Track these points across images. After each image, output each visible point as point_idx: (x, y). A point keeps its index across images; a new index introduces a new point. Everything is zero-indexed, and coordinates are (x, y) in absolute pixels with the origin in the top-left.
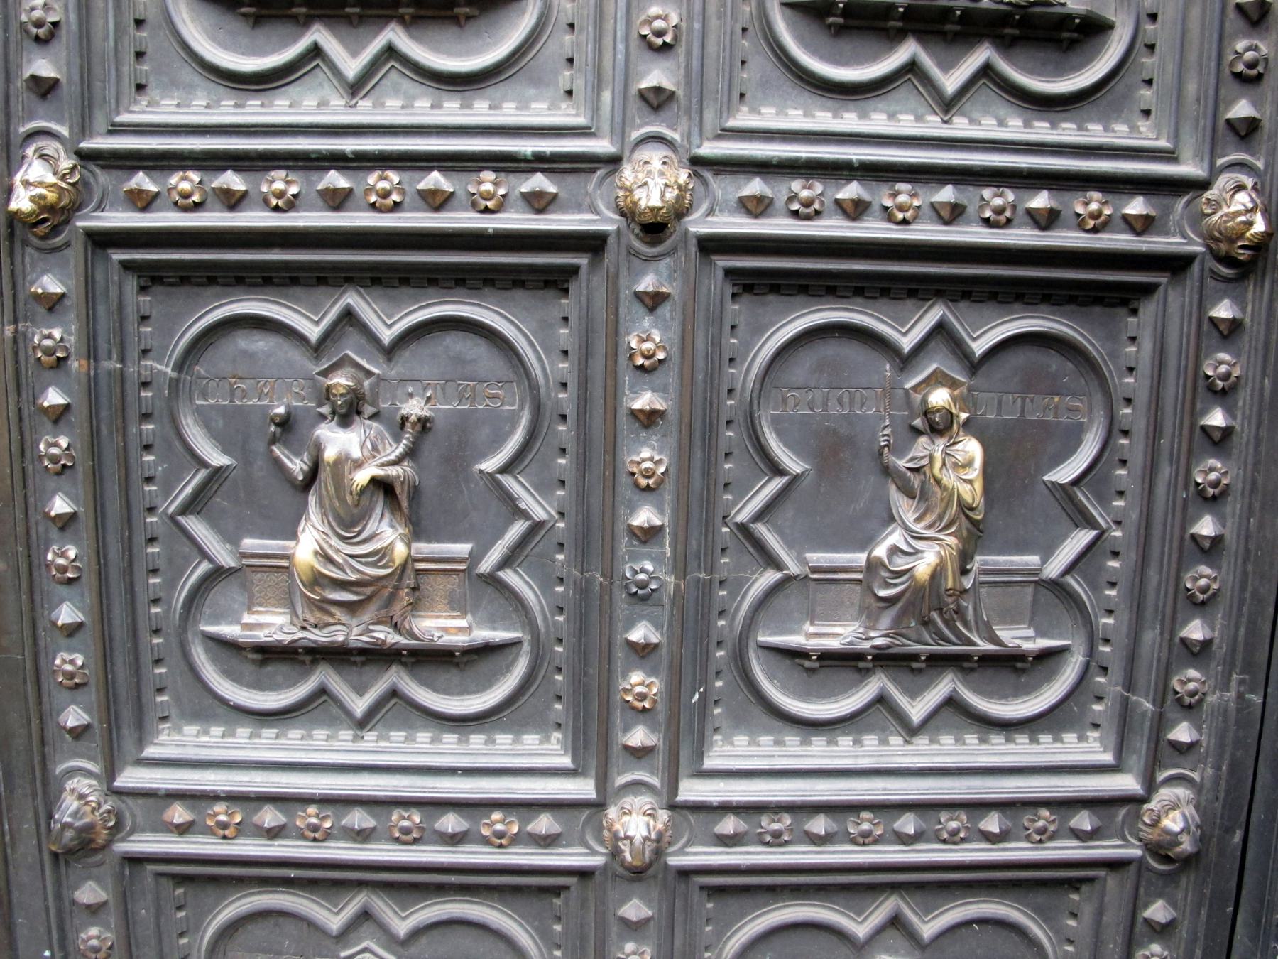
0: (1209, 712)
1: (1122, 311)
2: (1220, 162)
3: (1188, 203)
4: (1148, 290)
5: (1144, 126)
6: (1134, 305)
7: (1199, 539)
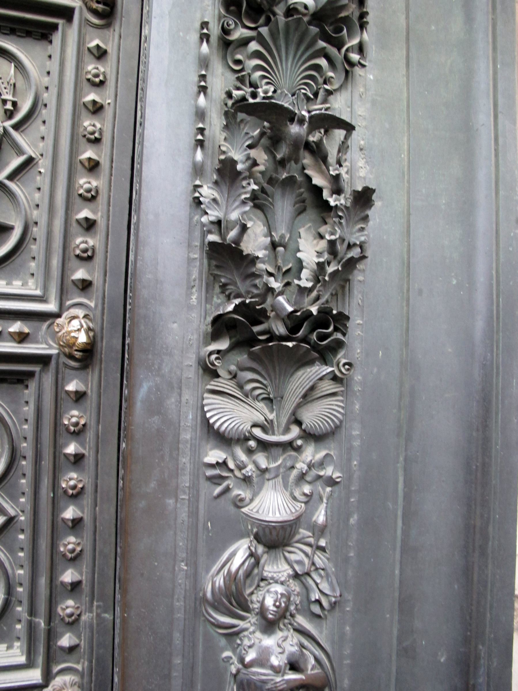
0: (84, 626)
1: (20, 386)
2: (69, 303)
3: (49, 326)
4: (31, 375)
5: (31, 282)
6: (26, 383)
7: (65, 521)
